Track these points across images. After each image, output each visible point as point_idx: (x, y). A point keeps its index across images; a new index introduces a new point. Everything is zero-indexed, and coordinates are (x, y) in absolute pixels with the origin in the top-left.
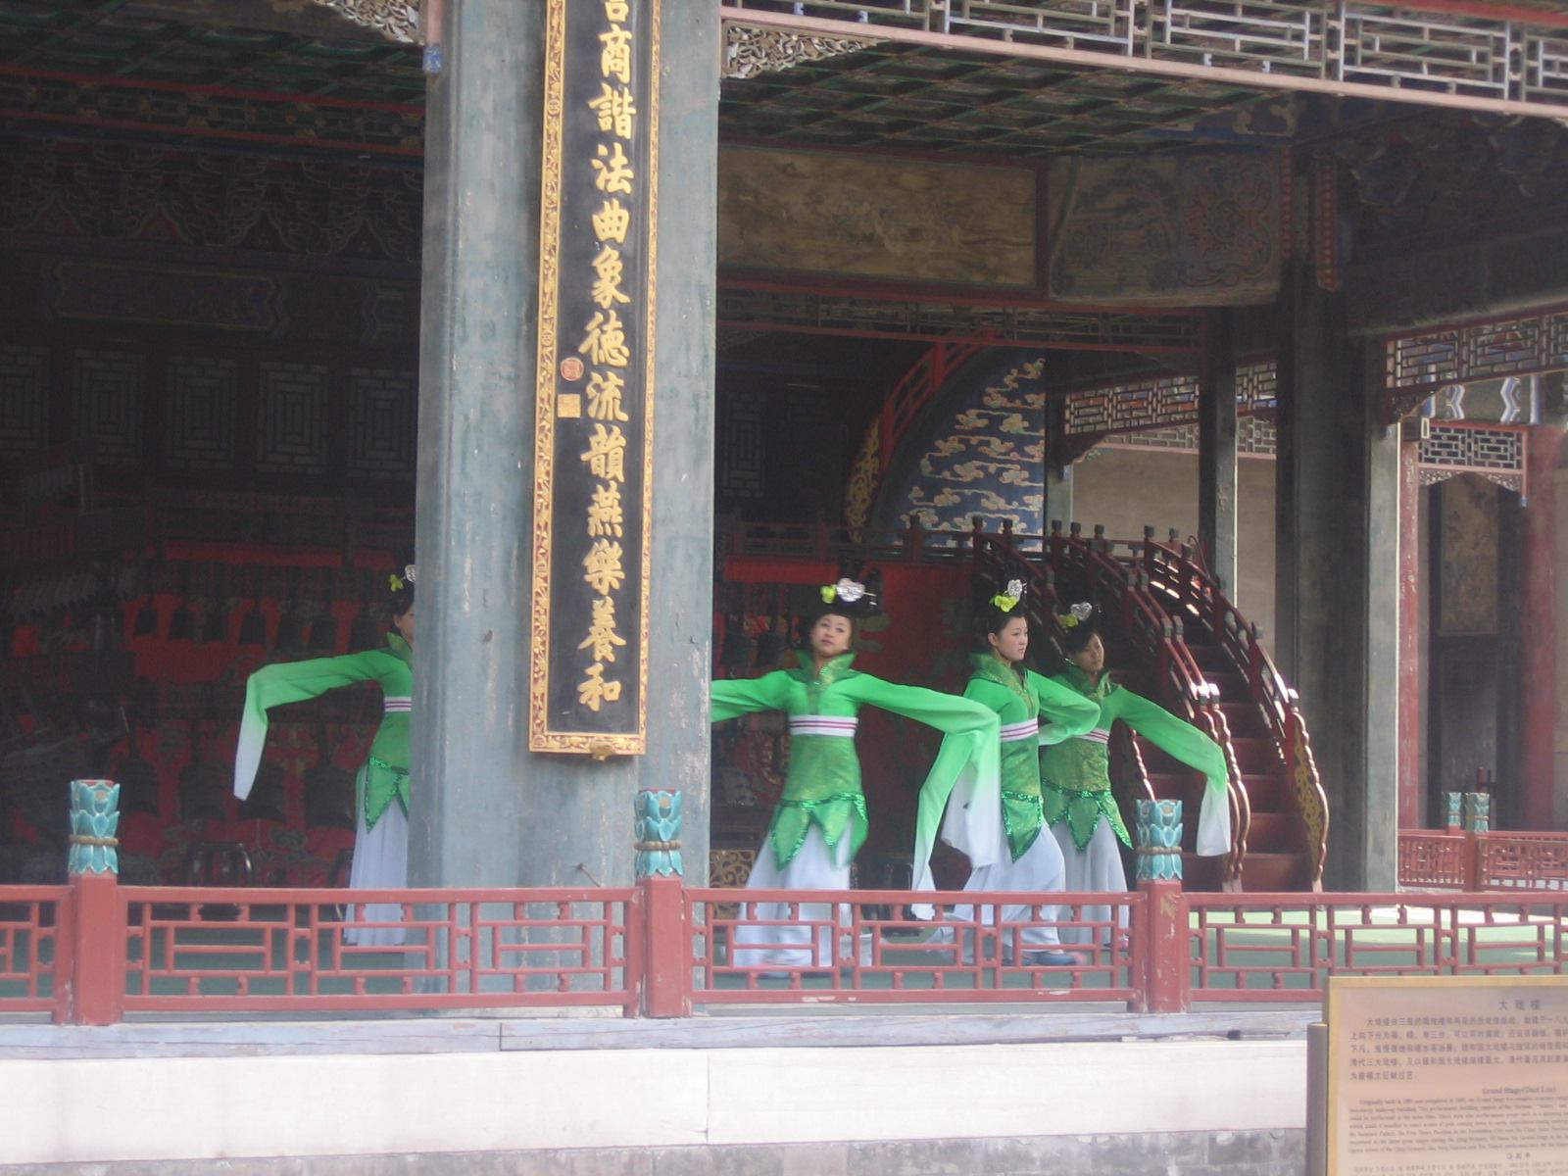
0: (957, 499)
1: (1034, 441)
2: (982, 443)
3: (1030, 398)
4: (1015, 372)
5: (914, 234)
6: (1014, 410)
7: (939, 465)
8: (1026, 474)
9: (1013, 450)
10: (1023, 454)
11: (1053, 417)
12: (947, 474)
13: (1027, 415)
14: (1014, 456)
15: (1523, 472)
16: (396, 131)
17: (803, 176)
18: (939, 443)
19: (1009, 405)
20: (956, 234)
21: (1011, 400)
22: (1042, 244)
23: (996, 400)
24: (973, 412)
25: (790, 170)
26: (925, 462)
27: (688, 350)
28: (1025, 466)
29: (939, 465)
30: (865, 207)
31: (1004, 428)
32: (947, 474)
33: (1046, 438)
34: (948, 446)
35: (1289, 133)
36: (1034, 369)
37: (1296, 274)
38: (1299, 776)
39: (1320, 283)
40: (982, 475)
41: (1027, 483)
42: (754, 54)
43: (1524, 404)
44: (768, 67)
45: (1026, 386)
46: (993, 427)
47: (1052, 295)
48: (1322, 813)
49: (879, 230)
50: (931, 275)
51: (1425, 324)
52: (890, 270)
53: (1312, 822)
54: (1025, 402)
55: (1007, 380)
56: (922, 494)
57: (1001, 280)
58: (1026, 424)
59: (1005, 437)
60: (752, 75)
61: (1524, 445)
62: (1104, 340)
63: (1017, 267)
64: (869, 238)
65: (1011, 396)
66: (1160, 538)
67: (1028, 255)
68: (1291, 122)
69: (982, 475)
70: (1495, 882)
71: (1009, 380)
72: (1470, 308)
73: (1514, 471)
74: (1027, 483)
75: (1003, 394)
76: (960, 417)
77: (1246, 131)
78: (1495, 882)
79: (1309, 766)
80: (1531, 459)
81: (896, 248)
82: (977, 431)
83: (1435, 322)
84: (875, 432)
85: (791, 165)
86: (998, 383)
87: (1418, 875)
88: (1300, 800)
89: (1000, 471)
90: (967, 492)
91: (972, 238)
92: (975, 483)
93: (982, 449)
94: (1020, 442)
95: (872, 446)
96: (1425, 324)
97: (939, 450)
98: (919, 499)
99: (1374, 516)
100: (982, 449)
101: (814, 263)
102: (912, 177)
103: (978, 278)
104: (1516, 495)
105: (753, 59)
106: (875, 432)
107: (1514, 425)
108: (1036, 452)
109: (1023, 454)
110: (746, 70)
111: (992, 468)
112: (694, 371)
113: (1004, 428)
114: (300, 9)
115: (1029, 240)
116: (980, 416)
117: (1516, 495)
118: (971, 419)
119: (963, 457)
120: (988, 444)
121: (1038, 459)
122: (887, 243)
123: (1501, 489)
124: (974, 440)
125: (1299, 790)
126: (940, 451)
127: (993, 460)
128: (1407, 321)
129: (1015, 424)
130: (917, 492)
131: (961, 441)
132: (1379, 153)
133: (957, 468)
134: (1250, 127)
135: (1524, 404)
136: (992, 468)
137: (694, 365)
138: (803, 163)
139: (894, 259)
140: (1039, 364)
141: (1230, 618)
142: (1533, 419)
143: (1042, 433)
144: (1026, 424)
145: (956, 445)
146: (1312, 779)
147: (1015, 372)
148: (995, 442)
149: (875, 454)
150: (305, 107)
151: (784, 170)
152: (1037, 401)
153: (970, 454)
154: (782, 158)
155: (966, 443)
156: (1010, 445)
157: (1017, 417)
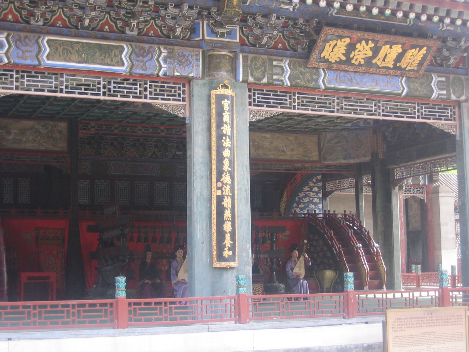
0: (304, 206)
1: (320, 193)
2: (308, 194)
3: (319, 183)
4: (315, 178)
5: (292, 150)
6: (316, 186)
7: (300, 199)
8: (318, 200)
9: (315, 195)
10: (318, 195)
11: (324, 187)
12: (301, 201)
13: (318, 187)
14: (316, 196)
15: (425, 195)
16: (181, 132)
17: (268, 138)
18: (300, 194)
19: (314, 185)
21: (315, 184)
22: (320, 151)
23: (311, 184)
24: (306, 187)
25: (265, 137)
26: (297, 198)
27: (244, 180)
28: (318, 198)
29: (300, 198)
30: (281, 145)
31: (313, 190)
32: (301, 201)
33: (322, 192)
34: (302, 195)
35: (371, 125)
36: (319, 177)
37: (374, 155)
38: (380, 263)
39: (379, 157)
40: (309, 200)
41: (319, 202)
42: (256, 116)
43: (425, 180)
44: (259, 119)
45: (318, 181)
46: (311, 190)
47: (322, 162)
48: (385, 271)
49: (285, 149)
50: (297, 159)
51: (403, 165)
52: (288, 158)
53: (383, 273)
54: (317, 184)
55: (313, 180)
56: (296, 205)
57: (311, 159)
58: (318, 189)
59: (313, 192)
60: (256, 120)
62: (334, 171)
63: (315, 156)
64: (283, 151)
65: (314, 183)
66: (348, 213)
67: (317, 153)
69: (309, 200)
71: (314, 180)
72: (412, 161)
73: (423, 195)
74: (319, 202)
75: (313, 183)
76: (304, 188)
77: (362, 125)
79: (381, 261)
81: (289, 153)
82: (308, 191)
83: (404, 164)
84: (286, 192)
85: (266, 136)
86: (312, 181)
88: (380, 268)
89: (313, 199)
90: (306, 204)
91: (304, 150)
92: (308, 202)
93: (309, 195)
94: (317, 193)
95: (285, 195)
97: (300, 196)
98: (296, 206)
99: (393, 206)
100: (309, 195)
101: (271, 157)
102: (291, 137)
103: (306, 159)
104: (424, 200)
105: (256, 117)
106: (286, 192)
107: (422, 185)
108: (320, 195)
109: (318, 195)
110: (254, 119)
111: (311, 199)
112: (245, 184)
113: (313, 190)
115: (317, 150)
116: (308, 188)
117: (424, 200)
118: (306, 188)
119: (305, 197)
120: (310, 194)
121: (321, 197)
122: (286, 151)
123: (420, 199)
124: (307, 193)
125: (380, 266)
126: (300, 196)
127: (311, 197)
128: (399, 164)
129: (316, 189)
130: (295, 205)
131: (304, 193)
132: (391, 129)
133: (304, 199)
134: (363, 124)
135: (425, 180)
136: (311, 199)
137: (245, 182)
138: (268, 136)
139: (288, 155)
140: (320, 176)
141: (363, 229)
142: (427, 184)
143: (322, 191)
144: (318, 189)
145: (303, 194)
146: (382, 264)
147: (315, 178)
148: (312, 193)
150: (162, 128)
151: (264, 137)
152: (320, 184)
153: (307, 196)
154: (264, 135)
155: (305, 193)
156: (315, 194)
157: (316, 188)
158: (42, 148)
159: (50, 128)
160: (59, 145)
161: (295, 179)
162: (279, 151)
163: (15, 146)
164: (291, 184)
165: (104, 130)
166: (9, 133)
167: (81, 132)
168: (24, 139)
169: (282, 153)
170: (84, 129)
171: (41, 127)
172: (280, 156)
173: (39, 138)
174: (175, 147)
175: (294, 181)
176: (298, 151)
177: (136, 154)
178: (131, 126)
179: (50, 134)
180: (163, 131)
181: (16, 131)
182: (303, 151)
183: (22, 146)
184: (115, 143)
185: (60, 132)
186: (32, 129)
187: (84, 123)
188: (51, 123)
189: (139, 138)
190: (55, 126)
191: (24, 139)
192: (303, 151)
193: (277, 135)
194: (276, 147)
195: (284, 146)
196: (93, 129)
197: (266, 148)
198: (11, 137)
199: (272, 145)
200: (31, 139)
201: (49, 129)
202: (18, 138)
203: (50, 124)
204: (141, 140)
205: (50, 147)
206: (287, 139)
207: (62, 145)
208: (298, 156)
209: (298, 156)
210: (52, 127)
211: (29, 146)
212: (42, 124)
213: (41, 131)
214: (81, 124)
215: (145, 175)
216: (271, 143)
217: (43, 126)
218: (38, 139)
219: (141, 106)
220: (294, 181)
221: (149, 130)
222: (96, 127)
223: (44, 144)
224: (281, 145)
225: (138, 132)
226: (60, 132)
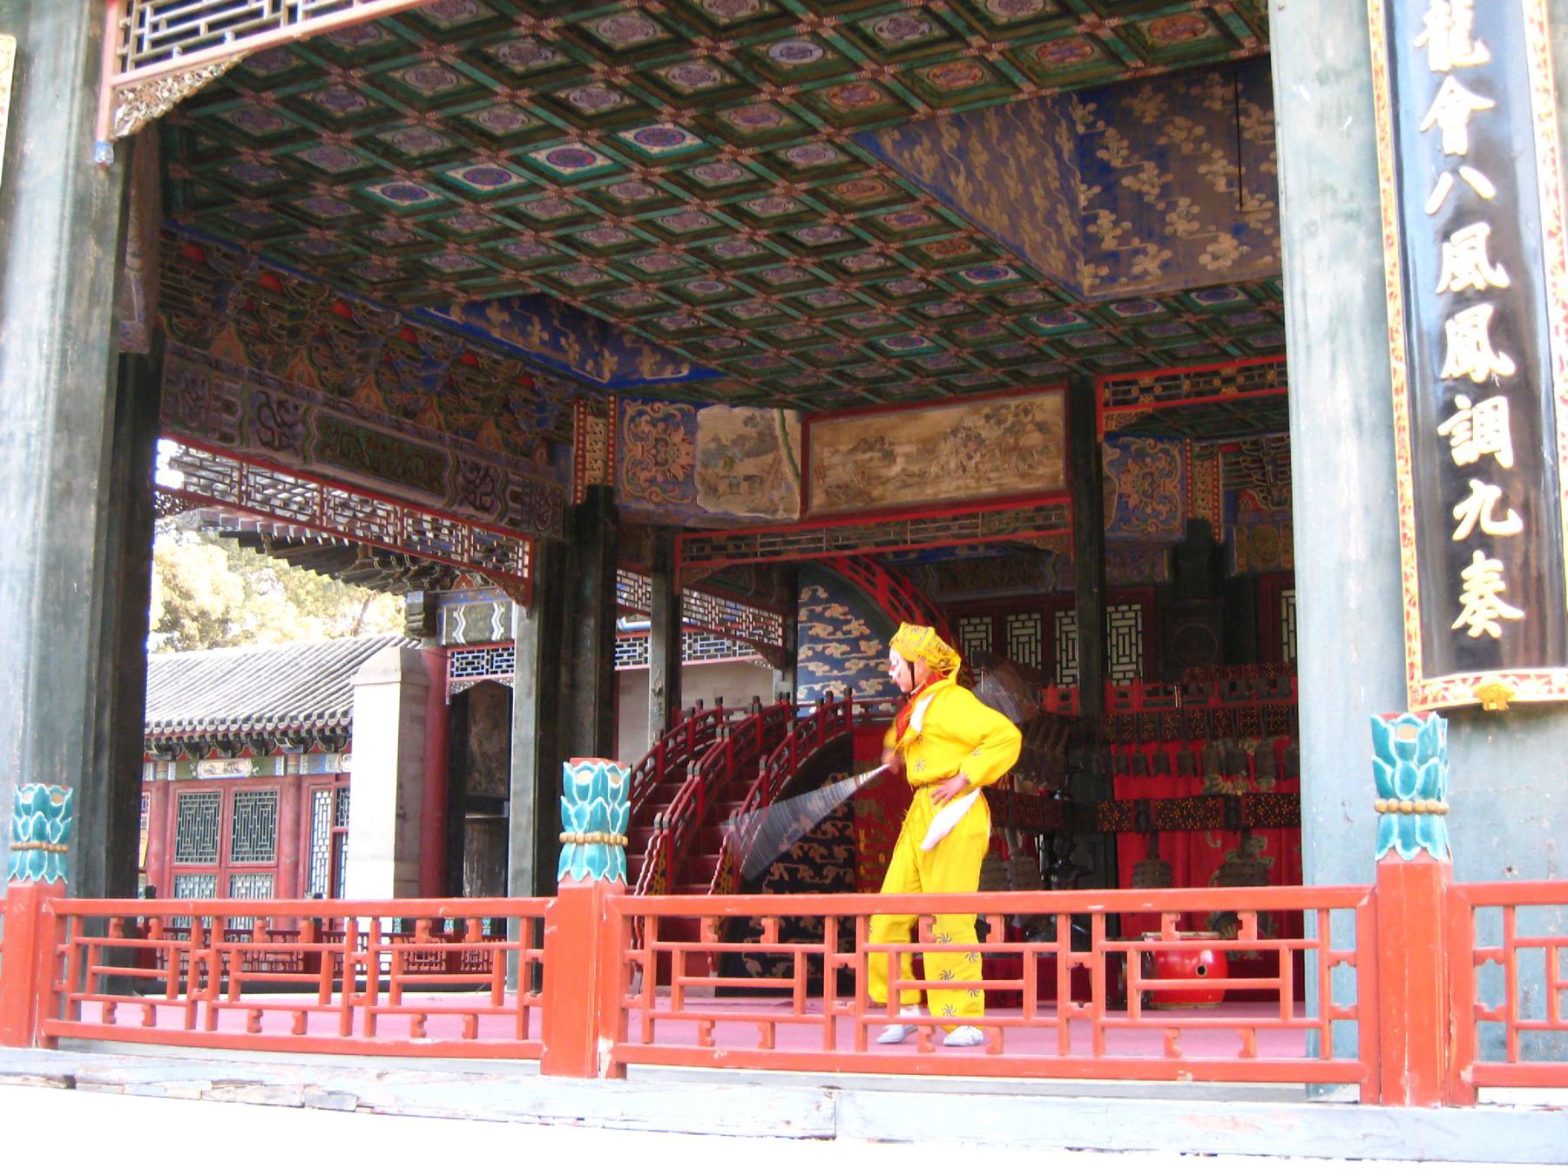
158: (988, 490)
159: (1011, 419)
160: (1041, 471)
163: (908, 496)
165: (1188, 396)
166: (889, 457)
167: (1105, 414)
168: (934, 470)
170: (1117, 403)
171: (982, 422)
173: (977, 457)
179: (1011, 441)
181: (907, 448)
183: (928, 493)
185: (1041, 427)
186: (955, 432)
187: (1115, 384)
188: (1013, 403)
190: (1026, 412)
191: (934, 470)
196: (1146, 399)
198: (896, 469)
200: (952, 465)
201: (1008, 424)
202: (915, 468)
203: (1008, 407)
205: (1013, 482)
207: (1049, 471)
210: (1017, 415)
211: (949, 489)
212: (986, 410)
213: (984, 434)
214: (1107, 386)
217: (988, 417)
218: (973, 462)
219: (1159, 272)
222: (1158, 390)
223: (991, 475)
226: (1041, 427)
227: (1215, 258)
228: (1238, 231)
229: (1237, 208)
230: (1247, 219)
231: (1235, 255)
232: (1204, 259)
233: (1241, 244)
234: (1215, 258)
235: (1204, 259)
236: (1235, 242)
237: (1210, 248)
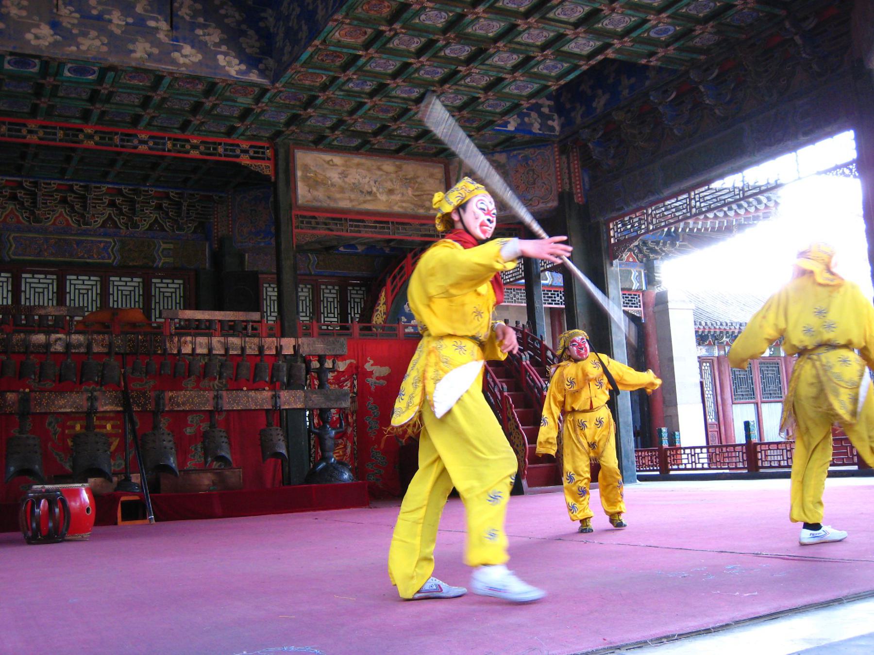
5: (391, 192)
15: (642, 309)
16: (136, 142)
17: (336, 165)
20: (410, 192)
30: (367, 179)
43: (640, 282)
49: (374, 189)
50: (400, 210)
51: (631, 208)
52: (381, 207)
61: (641, 298)
64: (370, 193)
68: (557, 128)
70: (675, 467)
72: (653, 194)
77: (538, 131)
78: (675, 467)
80: (644, 304)
81: (383, 198)
83: (634, 206)
84: (383, 294)
87: (649, 466)
91: (417, 193)
95: (382, 299)
96: (631, 208)
101: (344, 204)
102: (389, 166)
103: (421, 211)
106: (383, 294)
107: (637, 290)
114: (47, 44)
117: (640, 318)
122: (378, 195)
130: (404, 319)
132: (601, 133)
134: (540, 130)
135: (640, 282)
138: (338, 160)
139: (382, 203)
141: (549, 354)
142: (644, 288)
149: (384, 304)
151: (328, 162)
154: (328, 157)
161: (402, 268)
162: (362, 192)
164: (395, 278)
169: (369, 198)
172: (365, 202)
174: (152, 206)
175: (399, 273)
176: (403, 194)
177: (69, 219)
178: (10, 124)
180: (90, 137)
182: (415, 196)
184: (19, 195)
189: (71, 183)
192: (415, 196)
193: (356, 160)
194: (354, 184)
195: (372, 183)
197: (333, 185)
199: (346, 179)
204: (75, 188)
206: (379, 169)
208: (404, 205)
209: (404, 205)
215: (88, 260)
216: (344, 175)
220: (399, 273)
221: (55, 134)
224: (367, 179)
225: (29, 136)
227: (37, 37)
228: (55, 25)
229: (55, 11)
230: (61, 19)
231: (51, 40)
232: (29, 36)
233: (55, 34)
234: (37, 37)
235: (29, 36)
236: (52, 32)
237: (33, 31)
